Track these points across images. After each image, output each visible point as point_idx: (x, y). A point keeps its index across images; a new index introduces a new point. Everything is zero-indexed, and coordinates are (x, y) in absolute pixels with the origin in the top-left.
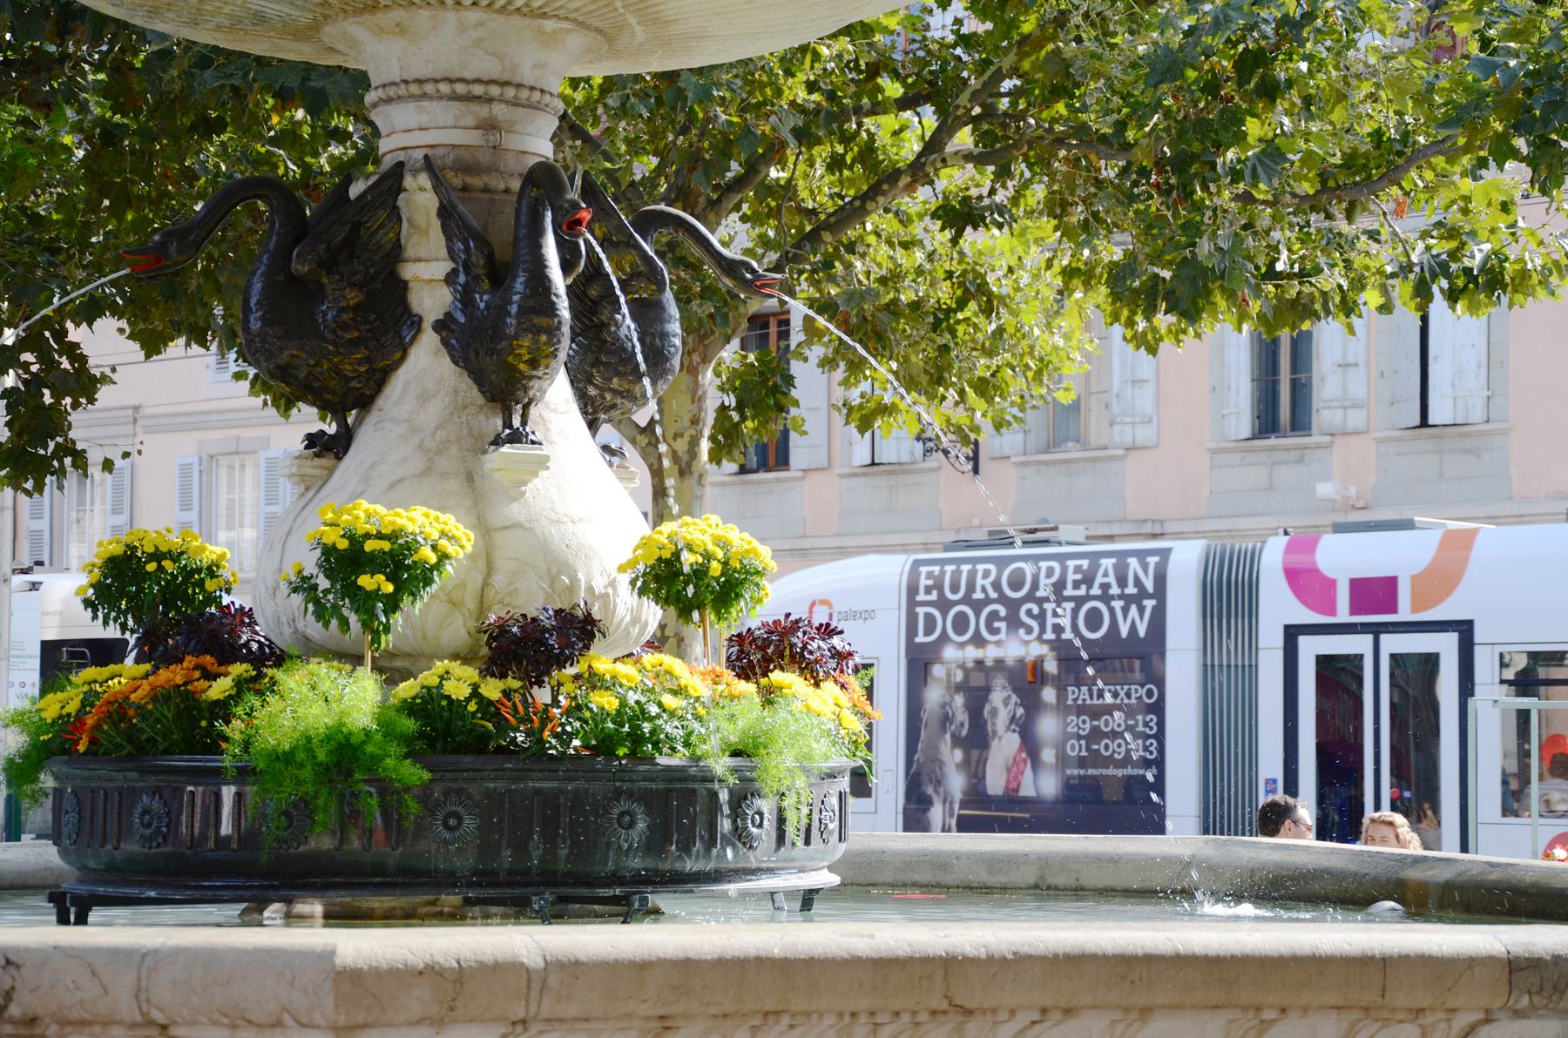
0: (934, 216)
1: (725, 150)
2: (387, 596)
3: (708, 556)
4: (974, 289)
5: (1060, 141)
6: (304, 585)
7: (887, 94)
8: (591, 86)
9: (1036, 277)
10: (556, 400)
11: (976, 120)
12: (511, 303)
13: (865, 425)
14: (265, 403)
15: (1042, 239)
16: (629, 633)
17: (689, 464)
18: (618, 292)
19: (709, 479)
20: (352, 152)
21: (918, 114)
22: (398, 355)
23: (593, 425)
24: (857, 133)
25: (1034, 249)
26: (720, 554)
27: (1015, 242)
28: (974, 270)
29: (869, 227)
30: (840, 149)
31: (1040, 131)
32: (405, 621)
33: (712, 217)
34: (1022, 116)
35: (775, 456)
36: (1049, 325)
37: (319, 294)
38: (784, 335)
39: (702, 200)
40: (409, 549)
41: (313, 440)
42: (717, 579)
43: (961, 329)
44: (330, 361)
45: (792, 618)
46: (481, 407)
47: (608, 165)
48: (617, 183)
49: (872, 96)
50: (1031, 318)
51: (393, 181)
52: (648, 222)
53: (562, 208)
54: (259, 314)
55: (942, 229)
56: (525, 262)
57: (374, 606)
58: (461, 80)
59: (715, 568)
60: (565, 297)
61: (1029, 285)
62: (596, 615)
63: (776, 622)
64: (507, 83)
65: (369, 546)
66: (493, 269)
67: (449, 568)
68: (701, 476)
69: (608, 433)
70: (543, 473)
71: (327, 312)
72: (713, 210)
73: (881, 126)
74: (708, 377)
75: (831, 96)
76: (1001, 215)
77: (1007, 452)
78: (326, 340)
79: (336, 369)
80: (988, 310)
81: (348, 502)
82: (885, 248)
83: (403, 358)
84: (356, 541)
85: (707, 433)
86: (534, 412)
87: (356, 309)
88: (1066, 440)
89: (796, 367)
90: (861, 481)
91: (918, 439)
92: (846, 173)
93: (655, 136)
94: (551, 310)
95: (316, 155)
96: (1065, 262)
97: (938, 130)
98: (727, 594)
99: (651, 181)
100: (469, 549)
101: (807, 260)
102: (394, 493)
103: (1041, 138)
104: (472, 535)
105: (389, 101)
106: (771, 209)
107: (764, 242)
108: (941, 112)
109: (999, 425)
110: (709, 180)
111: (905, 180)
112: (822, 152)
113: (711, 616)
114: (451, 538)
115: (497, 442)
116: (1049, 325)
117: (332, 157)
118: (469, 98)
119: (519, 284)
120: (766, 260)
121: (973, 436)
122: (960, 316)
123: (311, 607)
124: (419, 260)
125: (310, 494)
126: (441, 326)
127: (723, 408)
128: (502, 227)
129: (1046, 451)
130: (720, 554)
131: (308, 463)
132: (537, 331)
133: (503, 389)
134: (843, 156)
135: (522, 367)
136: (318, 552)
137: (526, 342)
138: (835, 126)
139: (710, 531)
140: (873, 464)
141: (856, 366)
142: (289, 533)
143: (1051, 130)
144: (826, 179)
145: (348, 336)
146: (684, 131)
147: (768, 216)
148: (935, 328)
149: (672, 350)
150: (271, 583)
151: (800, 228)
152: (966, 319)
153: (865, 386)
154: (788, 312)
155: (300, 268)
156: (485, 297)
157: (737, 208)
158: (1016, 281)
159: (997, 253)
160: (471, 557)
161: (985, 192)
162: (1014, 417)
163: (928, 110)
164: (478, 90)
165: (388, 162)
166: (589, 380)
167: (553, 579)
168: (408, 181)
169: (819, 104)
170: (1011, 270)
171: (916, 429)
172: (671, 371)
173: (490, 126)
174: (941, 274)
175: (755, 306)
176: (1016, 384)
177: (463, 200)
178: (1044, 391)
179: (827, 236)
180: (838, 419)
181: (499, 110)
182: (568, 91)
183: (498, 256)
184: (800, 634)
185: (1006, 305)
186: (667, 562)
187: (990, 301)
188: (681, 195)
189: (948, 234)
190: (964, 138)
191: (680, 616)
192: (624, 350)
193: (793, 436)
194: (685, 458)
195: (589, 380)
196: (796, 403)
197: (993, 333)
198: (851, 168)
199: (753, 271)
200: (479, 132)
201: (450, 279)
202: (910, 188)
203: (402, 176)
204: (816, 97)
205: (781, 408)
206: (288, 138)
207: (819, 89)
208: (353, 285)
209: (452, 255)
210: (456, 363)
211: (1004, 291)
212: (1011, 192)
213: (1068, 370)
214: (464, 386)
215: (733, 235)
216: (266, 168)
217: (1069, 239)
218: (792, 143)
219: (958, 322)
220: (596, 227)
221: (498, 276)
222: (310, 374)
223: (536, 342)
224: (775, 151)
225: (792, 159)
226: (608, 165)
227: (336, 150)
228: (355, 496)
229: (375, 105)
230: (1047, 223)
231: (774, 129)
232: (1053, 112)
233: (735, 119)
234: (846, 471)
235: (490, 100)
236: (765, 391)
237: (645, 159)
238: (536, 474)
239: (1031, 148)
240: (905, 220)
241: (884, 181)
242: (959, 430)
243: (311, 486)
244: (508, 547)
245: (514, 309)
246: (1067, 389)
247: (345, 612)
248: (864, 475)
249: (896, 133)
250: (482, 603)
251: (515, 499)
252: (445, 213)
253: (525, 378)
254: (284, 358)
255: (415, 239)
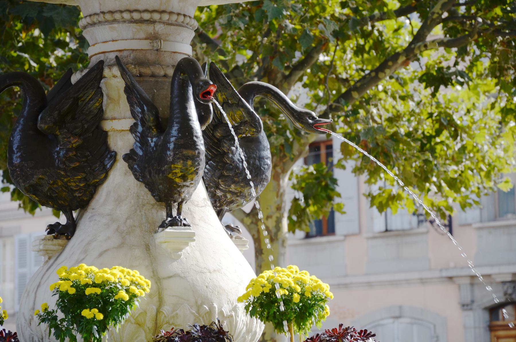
0: (421, 80)
1: (292, 46)
2: (100, 321)
3: (292, 291)
4: (445, 123)
5: (498, 31)
6: (48, 317)
7: (390, 7)
8: (211, 10)
9: (485, 114)
10: (198, 198)
11: (445, 21)
12: (169, 142)
13: (381, 208)
14: (20, 206)
15: (488, 92)
16: (245, 339)
17: (276, 234)
18: (233, 133)
19: (289, 242)
20: (69, 54)
21: (409, 19)
22: (103, 176)
23: (220, 214)
24: (372, 32)
25: (483, 97)
26: (299, 289)
27: (471, 93)
28: (446, 113)
29: (380, 88)
30: (362, 42)
31: (486, 26)
32: (110, 337)
33: (285, 85)
34: (474, 17)
35: (326, 227)
36: (493, 144)
37: (55, 141)
38: (330, 154)
39: (279, 76)
40: (112, 292)
41: (53, 229)
42: (297, 305)
43: (438, 148)
44: (62, 181)
45: (343, 327)
46: (153, 205)
47: (222, 58)
48: (227, 67)
49: (380, 9)
50: (483, 140)
51: (97, 72)
52: (249, 91)
53: (198, 85)
54: (19, 154)
55: (426, 87)
56: (177, 118)
57: (92, 328)
58: (137, 11)
59: (296, 298)
60: (201, 138)
61: (481, 120)
62: (225, 329)
63: (334, 330)
64: (163, 12)
65: (88, 291)
66: (158, 121)
67: (136, 303)
68: (283, 241)
69: (228, 217)
70: (192, 244)
71: (60, 152)
72: (286, 81)
73: (385, 27)
74: (286, 182)
75: (356, 11)
76: (462, 77)
77: (469, 221)
78: (59, 168)
79: (66, 186)
80: (455, 136)
81: (74, 265)
82: (390, 100)
83: (106, 177)
84: (80, 288)
85: (286, 215)
86: (185, 207)
87: (77, 149)
88: (507, 212)
89: (338, 173)
90: (379, 241)
91: (414, 214)
92: (366, 56)
93: (250, 38)
94: (193, 145)
95: (47, 56)
96: (503, 104)
97: (422, 28)
98: (304, 313)
99: (249, 65)
100: (148, 290)
101: (343, 110)
102: (102, 259)
103: (486, 30)
104: (150, 282)
105: (93, 24)
106: (321, 80)
107: (318, 100)
108: (423, 17)
109: (464, 206)
110: (283, 64)
111: (402, 59)
112: (351, 44)
113: (295, 328)
114: (137, 285)
115: (163, 225)
116: (493, 144)
117: (57, 58)
118: (141, 21)
119: (174, 131)
120: (318, 110)
121: (448, 213)
122: (438, 140)
123: (53, 330)
124: (114, 119)
125: (51, 262)
126: (128, 158)
127: (296, 200)
128: (163, 97)
129: (495, 219)
130: (299, 289)
131: (50, 242)
132: (186, 158)
133: (167, 194)
134: (363, 46)
135: (177, 180)
136: (57, 297)
137: (179, 165)
138: (358, 28)
139: (292, 276)
140: (387, 230)
141: (374, 172)
142: (39, 286)
143: (492, 25)
144: (353, 60)
145: (73, 165)
146: (267, 34)
147: (319, 83)
148: (422, 149)
149: (266, 167)
150: (28, 317)
151: (339, 91)
152: (442, 143)
153: (380, 183)
154: (331, 140)
155: (42, 126)
156: (154, 139)
157: (301, 79)
158: (472, 117)
159: (460, 101)
160: (150, 296)
161: (452, 64)
162: (474, 201)
163: (415, 15)
164: (146, 16)
165: (94, 61)
166: (217, 187)
167: (199, 307)
168: (106, 72)
169: (347, 16)
170: (469, 111)
171: (412, 209)
172: (266, 179)
173: (154, 37)
174: (424, 116)
175: (313, 137)
176: (475, 181)
177: (139, 82)
178: (491, 184)
179: (355, 95)
180: (365, 202)
181: (159, 28)
182: (197, 13)
183: (160, 115)
184: (349, 337)
185: (466, 132)
186: (267, 295)
187: (456, 131)
188: (266, 73)
189: (429, 91)
190: (438, 32)
191: (276, 328)
192: (237, 168)
193: (337, 215)
194: (273, 230)
195: (217, 187)
196: (339, 195)
197: (459, 150)
198: (368, 53)
199: (313, 118)
200: (148, 41)
201: (133, 129)
202: (405, 64)
203: (102, 69)
204: (346, 11)
205: (330, 199)
206: (31, 46)
207: (348, 6)
208: (75, 135)
209: (134, 115)
210: (138, 179)
211: (465, 123)
212: (468, 63)
213: (507, 170)
214: (143, 193)
215: (298, 96)
216: (17, 66)
217: (505, 91)
218: (331, 38)
219: (437, 144)
220: (219, 95)
221: (162, 127)
222: (50, 189)
223: (185, 165)
224: (322, 45)
225: (332, 49)
226: (222, 58)
227: (59, 52)
228: (79, 262)
229: (85, 27)
230: (491, 81)
231: (321, 32)
232: (493, 14)
233: (298, 27)
234: (370, 235)
235: (152, 22)
236: (320, 189)
237: (244, 52)
238: (187, 244)
239: (479, 36)
240: (402, 83)
241: (388, 60)
242: (439, 210)
243: (52, 257)
244: (171, 289)
245: (171, 146)
246: (507, 182)
247: (74, 332)
248: (381, 237)
249: (396, 31)
250: (156, 323)
251: (175, 260)
252: (129, 90)
253: (179, 186)
254: (34, 180)
255: (111, 106)
